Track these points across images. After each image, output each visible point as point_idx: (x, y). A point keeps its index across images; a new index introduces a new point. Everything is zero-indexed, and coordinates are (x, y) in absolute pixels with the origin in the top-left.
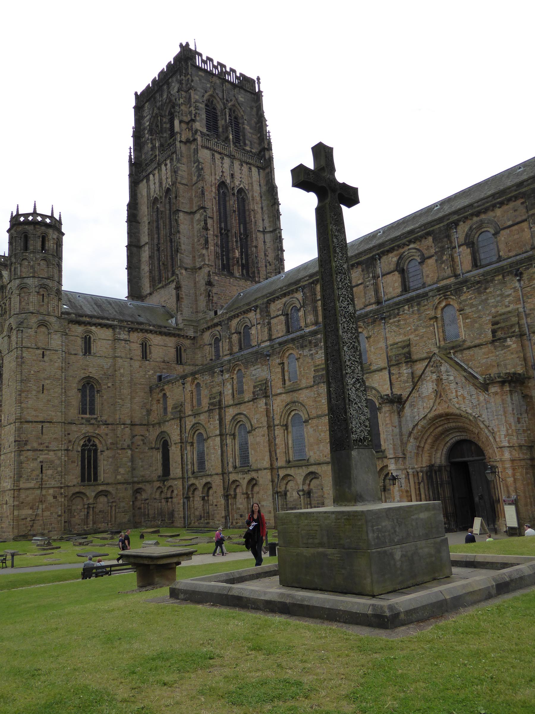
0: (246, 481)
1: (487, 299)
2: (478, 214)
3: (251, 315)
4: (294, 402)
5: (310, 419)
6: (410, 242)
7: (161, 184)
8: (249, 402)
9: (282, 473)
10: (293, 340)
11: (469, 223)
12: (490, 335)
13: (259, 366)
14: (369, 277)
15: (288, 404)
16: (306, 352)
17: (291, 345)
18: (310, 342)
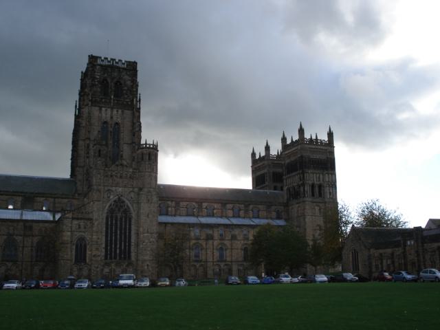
3: (169, 203)
7: (112, 118)
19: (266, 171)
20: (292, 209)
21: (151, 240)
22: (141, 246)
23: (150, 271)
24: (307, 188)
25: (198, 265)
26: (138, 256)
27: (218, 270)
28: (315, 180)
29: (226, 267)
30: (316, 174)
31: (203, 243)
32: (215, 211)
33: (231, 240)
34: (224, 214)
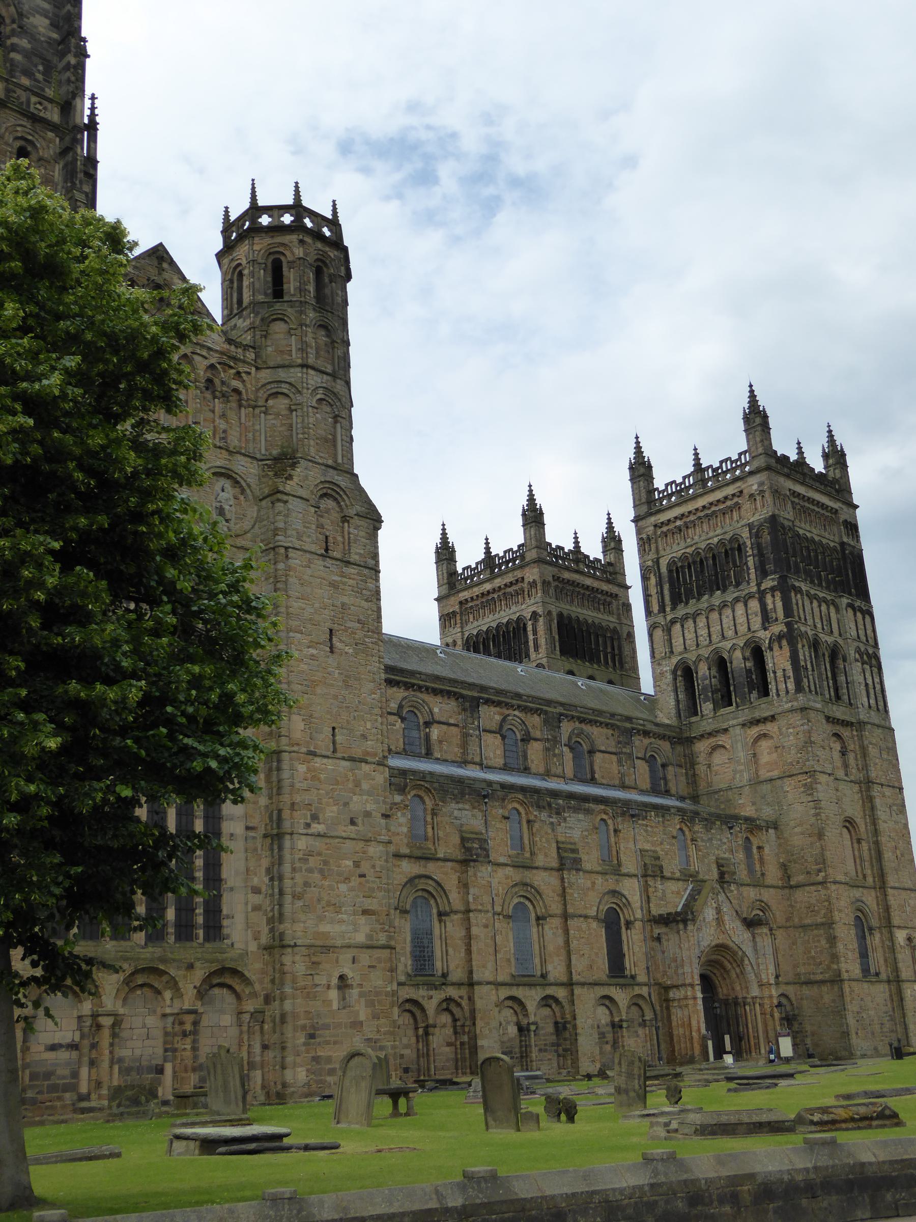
0: (434, 1002)
1: (711, 839)
2: (582, 721)
4: (526, 885)
5: (550, 916)
6: (519, 707)
8: (445, 860)
9: (504, 993)
10: (523, 789)
11: (571, 723)
12: (715, 874)
13: (467, 807)
14: (473, 723)
15: (516, 885)
16: (544, 815)
17: (520, 796)
18: (549, 805)
19: (526, 608)
20: (715, 748)
21: (358, 803)
22: (302, 843)
23: (357, 1025)
24: (804, 653)
25: (431, 1001)
26: (276, 919)
27: (513, 1030)
28: (819, 626)
29: (546, 1011)
30: (821, 601)
31: (447, 875)
32: (435, 732)
33: (561, 869)
34: (473, 749)
